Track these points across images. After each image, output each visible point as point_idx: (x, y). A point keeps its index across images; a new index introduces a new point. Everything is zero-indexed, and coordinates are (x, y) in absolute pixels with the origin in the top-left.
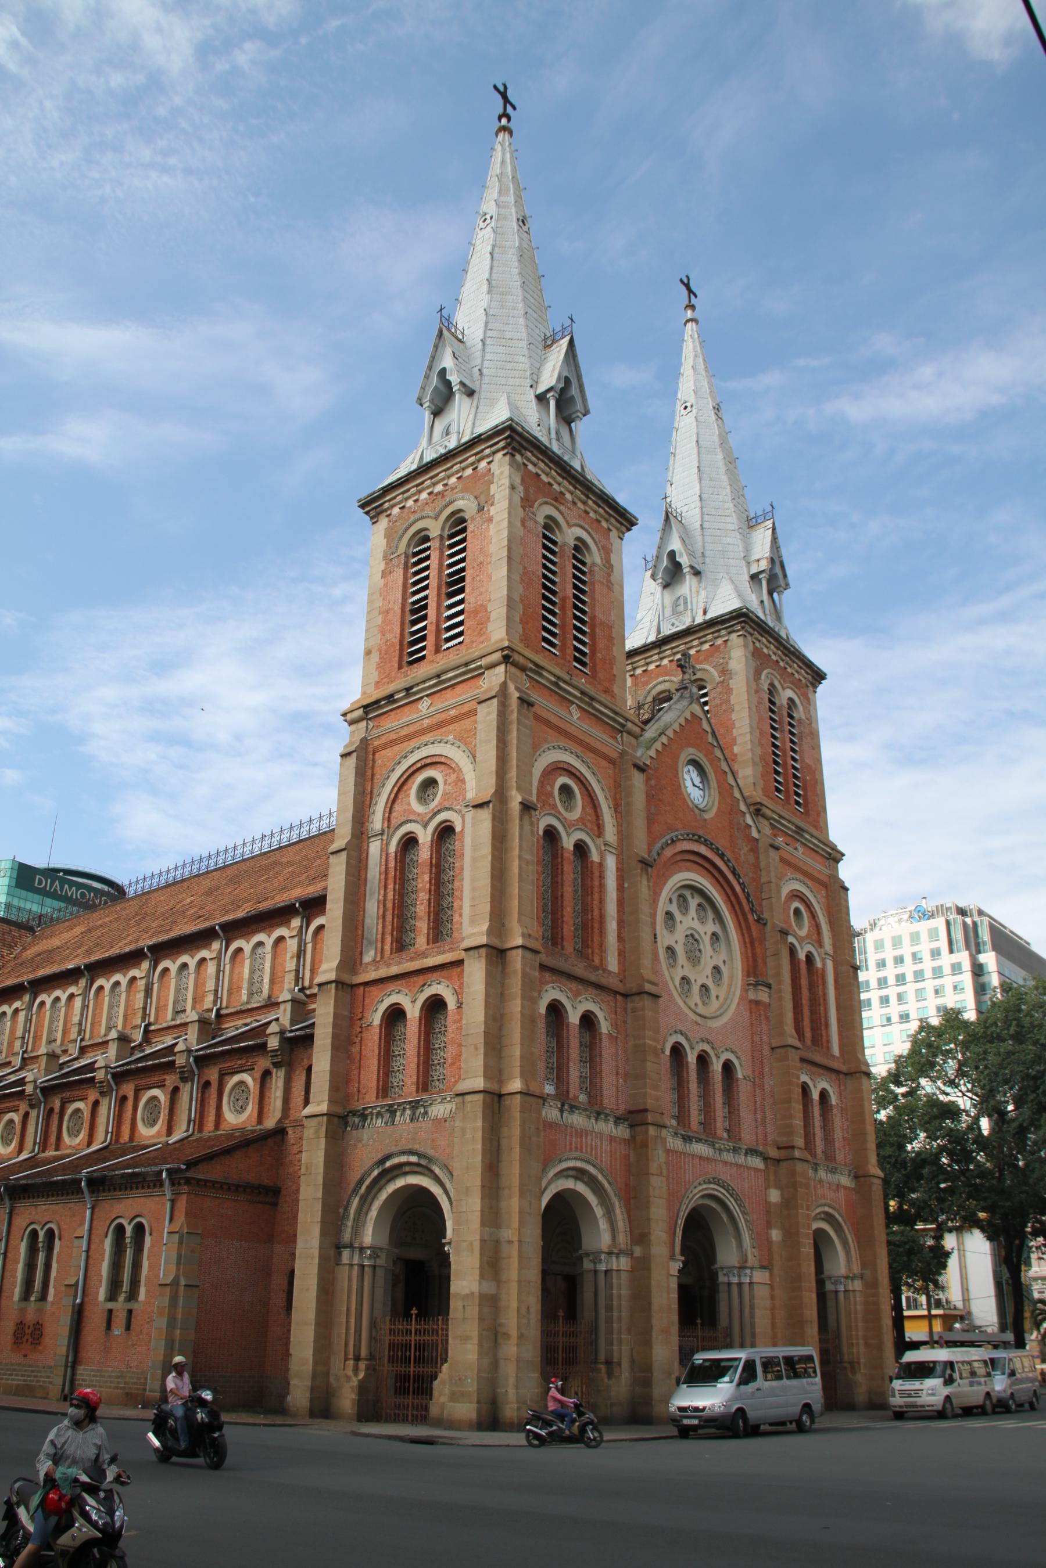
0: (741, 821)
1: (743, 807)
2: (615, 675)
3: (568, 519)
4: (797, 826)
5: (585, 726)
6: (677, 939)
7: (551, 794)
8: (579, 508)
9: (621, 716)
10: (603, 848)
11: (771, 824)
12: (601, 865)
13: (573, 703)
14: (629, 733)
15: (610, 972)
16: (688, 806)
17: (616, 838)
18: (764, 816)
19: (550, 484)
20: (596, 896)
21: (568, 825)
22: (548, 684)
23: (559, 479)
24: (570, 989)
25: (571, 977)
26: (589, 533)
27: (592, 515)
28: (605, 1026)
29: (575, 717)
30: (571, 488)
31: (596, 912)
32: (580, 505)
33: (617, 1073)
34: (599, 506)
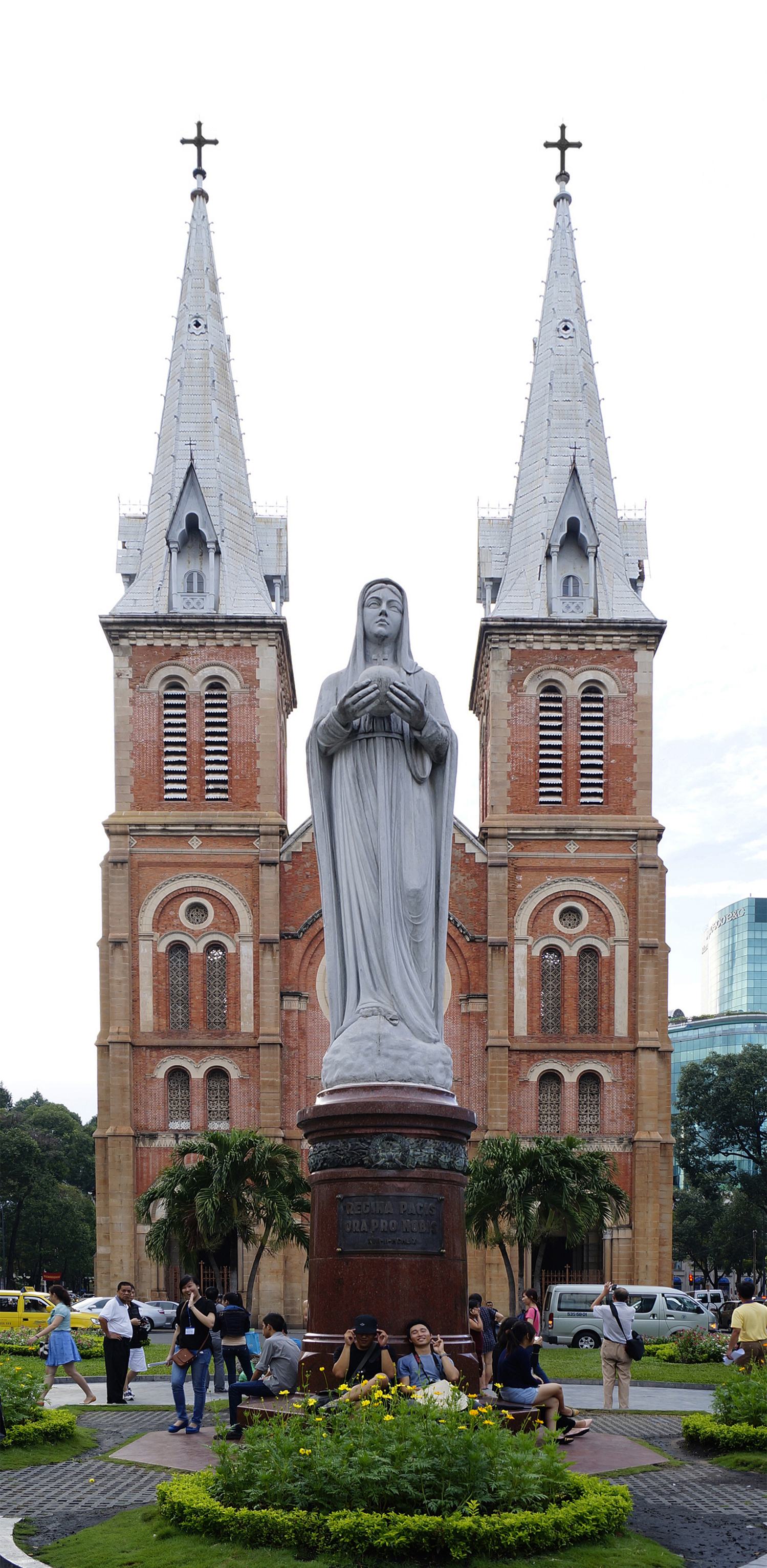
3: (190, 667)
4: (557, 829)
5: (206, 850)
7: (177, 917)
8: (209, 647)
9: (249, 825)
10: (238, 940)
11: (508, 839)
12: (237, 955)
13: (193, 836)
14: (266, 834)
15: (240, 1034)
17: (251, 928)
18: (494, 837)
19: (170, 645)
20: (233, 979)
21: (196, 936)
22: (160, 834)
23: (179, 634)
24: (192, 1056)
25: (189, 1047)
26: (221, 666)
27: (227, 643)
28: (234, 1074)
29: (195, 848)
30: (192, 634)
31: (232, 991)
32: (209, 643)
33: (250, 1105)
34: (232, 632)
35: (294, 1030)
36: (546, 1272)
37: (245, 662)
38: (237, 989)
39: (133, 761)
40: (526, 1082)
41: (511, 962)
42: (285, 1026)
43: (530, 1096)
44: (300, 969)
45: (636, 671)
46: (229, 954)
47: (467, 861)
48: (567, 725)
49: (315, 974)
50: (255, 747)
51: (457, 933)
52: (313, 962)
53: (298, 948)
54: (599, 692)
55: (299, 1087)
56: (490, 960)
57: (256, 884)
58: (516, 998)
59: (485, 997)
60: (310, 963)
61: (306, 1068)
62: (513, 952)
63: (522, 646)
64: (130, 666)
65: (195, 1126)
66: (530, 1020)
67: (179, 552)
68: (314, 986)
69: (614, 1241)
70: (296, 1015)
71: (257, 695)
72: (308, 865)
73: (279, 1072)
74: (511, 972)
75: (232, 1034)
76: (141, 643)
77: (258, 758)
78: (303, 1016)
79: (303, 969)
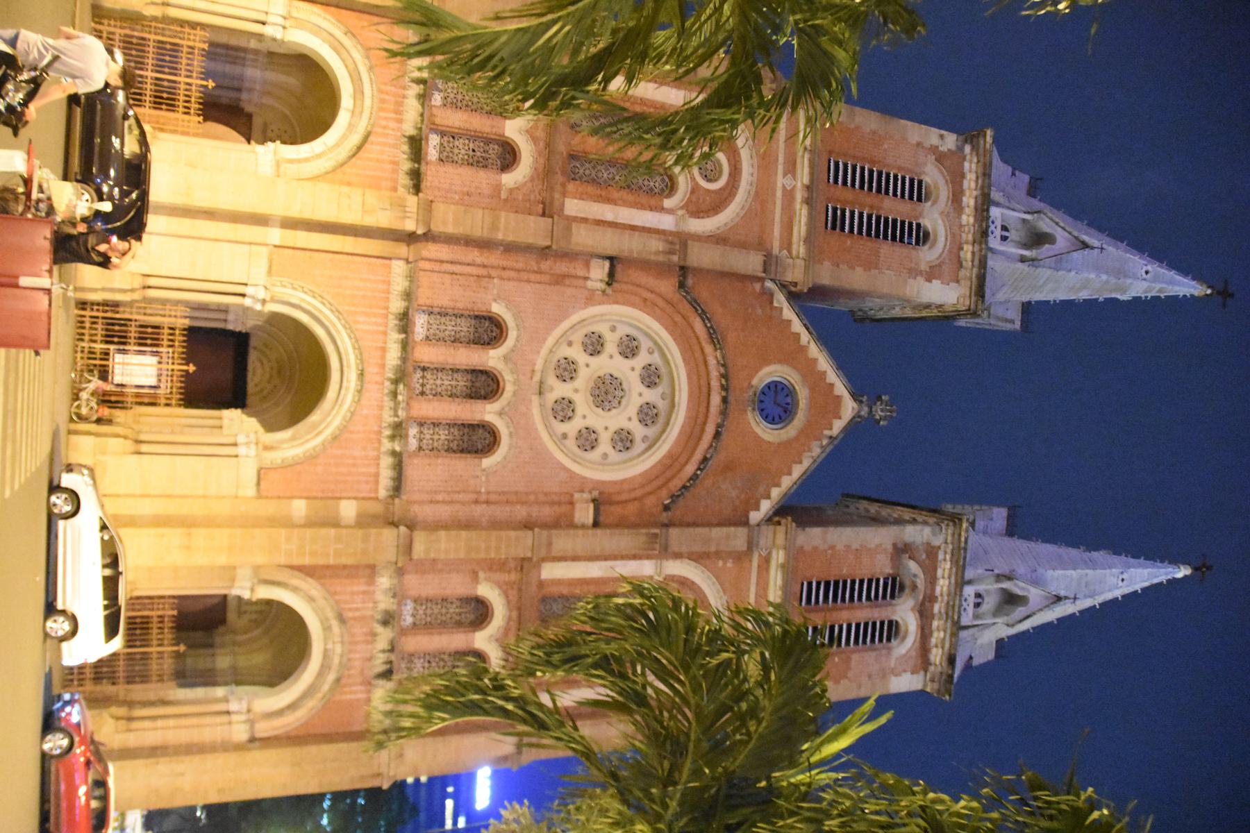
0: (761, 490)
1: (776, 493)
2: (838, 266)
5: (779, 193)
6: (610, 363)
12: (662, 209)
16: (751, 377)
20: (631, 198)
28: (509, 179)
31: (616, 195)
35: (562, 267)
36: (173, 616)
37: (946, 269)
38: (620, 202)
39: (868, 131)
40: (477, 583)
41: (635, 557)
42: (569, 255)
43: (456, 586)
44: (639, 286)
45: (912, 673)
46: (662, 200)
47: (752, 501)
48: (871, 607)
49: (633, 305)
50: (876, 268)
51: (673, 489)
52: (646, 305)
53: (667, 286)
54: (895, 639)
55: (485, 266)
56: (644, 531)
57: (743, 245)
58: (590, 564)
59: (596, 524)
60: (645, 300)
61: (509, 279)
62: (649, 557)
63: (941, 556)
64: (949, 150)
65: (435, 111)
66: (559, 582)
67: (1024, 220)
68: (617, 303)
69: (225, 718)
70: (581, 272)
71: (919, 278)
72: (759, 311)
73: (510, 238)
74: (623, 557)
75: (563, 185)
76: (966, 165)
77: (865, 270)
78: (581, 282)
79: (640, 291)
